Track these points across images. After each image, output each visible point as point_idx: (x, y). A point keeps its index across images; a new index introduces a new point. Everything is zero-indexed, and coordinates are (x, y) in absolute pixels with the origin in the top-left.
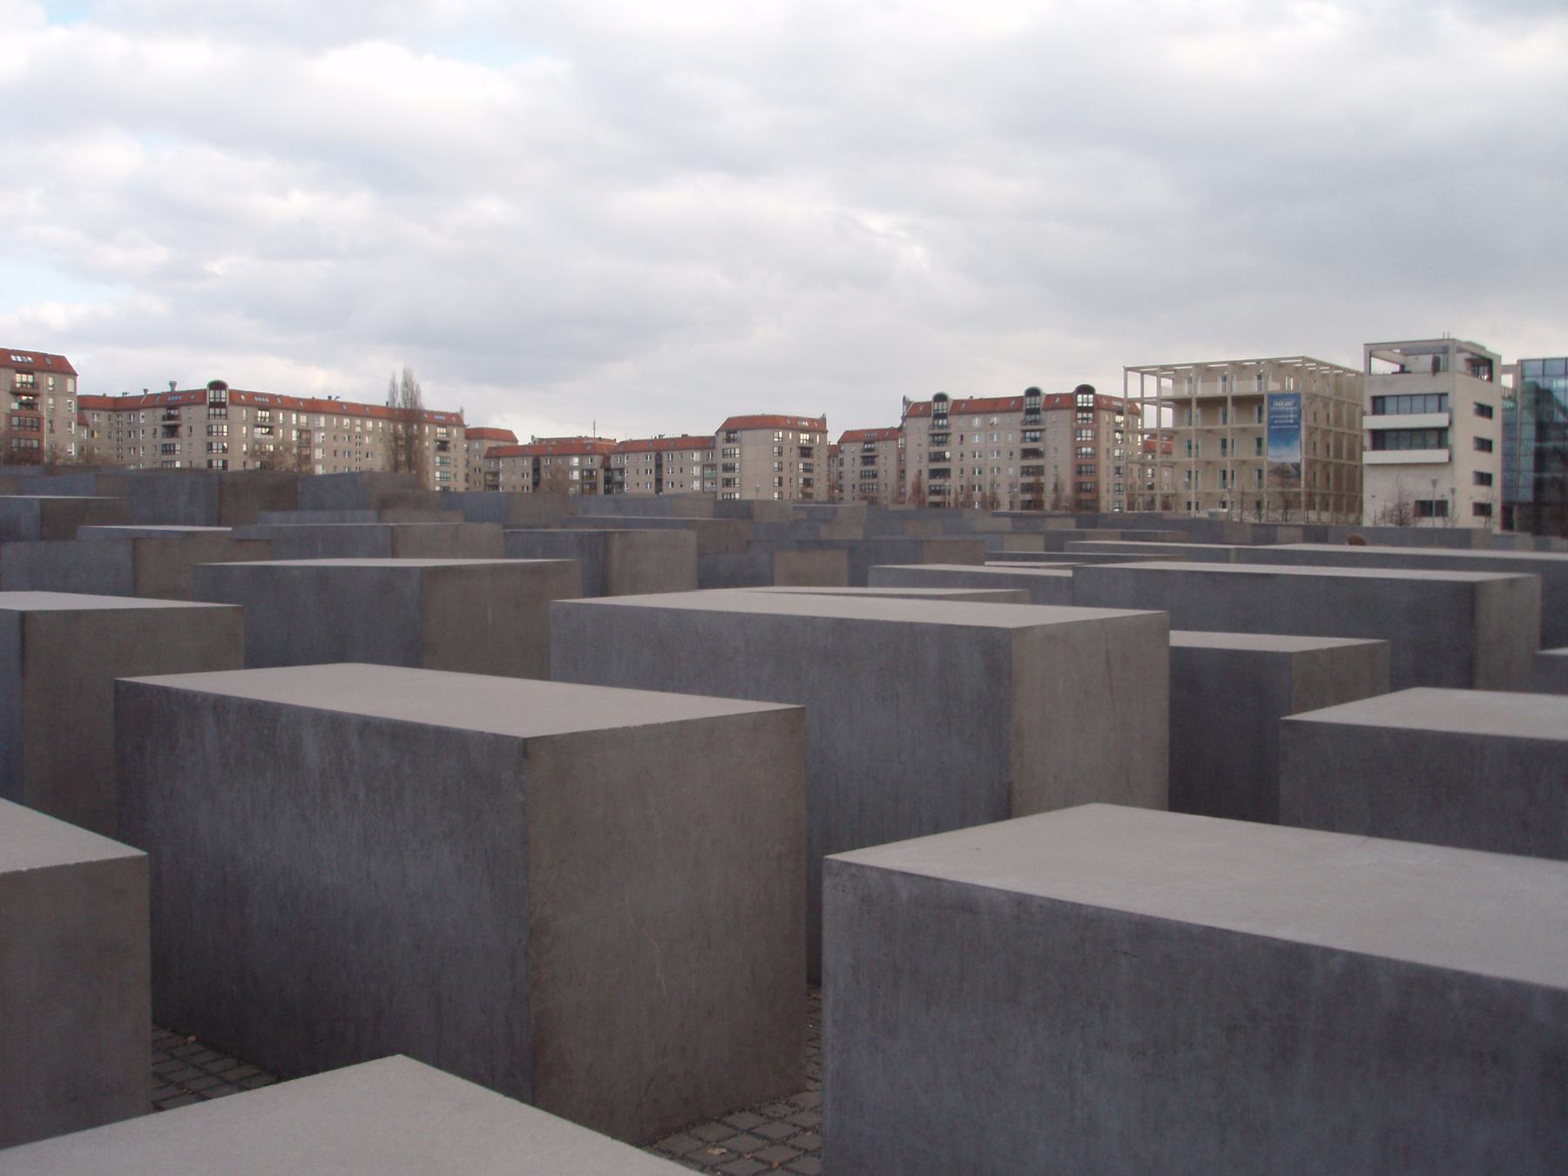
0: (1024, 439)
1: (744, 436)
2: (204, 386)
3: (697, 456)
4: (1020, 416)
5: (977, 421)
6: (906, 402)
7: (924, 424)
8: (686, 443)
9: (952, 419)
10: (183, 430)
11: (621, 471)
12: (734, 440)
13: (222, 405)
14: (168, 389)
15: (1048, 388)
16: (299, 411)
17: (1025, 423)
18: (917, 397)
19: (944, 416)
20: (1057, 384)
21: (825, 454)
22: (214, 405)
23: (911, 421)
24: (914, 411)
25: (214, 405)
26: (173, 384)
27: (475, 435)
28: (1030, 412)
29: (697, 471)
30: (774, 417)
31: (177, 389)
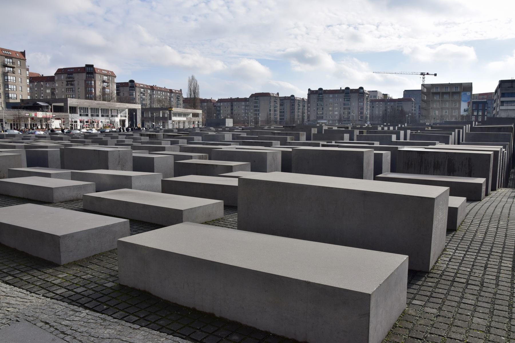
0: (345, 101)
2: (128, 81)
3: (243, 103)
4: (344, 94)
5: (331, 96)
6: (309, 90)
7: (315, 96)
8: (238, 100)
9: (324, 95)
11: (220, 107)
13: (133, 87)
15: (351, 88)
17: (345, 96)
18: (312, 89)
19: (321, 94)
23: (311, 95)
24: (311, 93)
25: (131, 87)
30: (263, 93)
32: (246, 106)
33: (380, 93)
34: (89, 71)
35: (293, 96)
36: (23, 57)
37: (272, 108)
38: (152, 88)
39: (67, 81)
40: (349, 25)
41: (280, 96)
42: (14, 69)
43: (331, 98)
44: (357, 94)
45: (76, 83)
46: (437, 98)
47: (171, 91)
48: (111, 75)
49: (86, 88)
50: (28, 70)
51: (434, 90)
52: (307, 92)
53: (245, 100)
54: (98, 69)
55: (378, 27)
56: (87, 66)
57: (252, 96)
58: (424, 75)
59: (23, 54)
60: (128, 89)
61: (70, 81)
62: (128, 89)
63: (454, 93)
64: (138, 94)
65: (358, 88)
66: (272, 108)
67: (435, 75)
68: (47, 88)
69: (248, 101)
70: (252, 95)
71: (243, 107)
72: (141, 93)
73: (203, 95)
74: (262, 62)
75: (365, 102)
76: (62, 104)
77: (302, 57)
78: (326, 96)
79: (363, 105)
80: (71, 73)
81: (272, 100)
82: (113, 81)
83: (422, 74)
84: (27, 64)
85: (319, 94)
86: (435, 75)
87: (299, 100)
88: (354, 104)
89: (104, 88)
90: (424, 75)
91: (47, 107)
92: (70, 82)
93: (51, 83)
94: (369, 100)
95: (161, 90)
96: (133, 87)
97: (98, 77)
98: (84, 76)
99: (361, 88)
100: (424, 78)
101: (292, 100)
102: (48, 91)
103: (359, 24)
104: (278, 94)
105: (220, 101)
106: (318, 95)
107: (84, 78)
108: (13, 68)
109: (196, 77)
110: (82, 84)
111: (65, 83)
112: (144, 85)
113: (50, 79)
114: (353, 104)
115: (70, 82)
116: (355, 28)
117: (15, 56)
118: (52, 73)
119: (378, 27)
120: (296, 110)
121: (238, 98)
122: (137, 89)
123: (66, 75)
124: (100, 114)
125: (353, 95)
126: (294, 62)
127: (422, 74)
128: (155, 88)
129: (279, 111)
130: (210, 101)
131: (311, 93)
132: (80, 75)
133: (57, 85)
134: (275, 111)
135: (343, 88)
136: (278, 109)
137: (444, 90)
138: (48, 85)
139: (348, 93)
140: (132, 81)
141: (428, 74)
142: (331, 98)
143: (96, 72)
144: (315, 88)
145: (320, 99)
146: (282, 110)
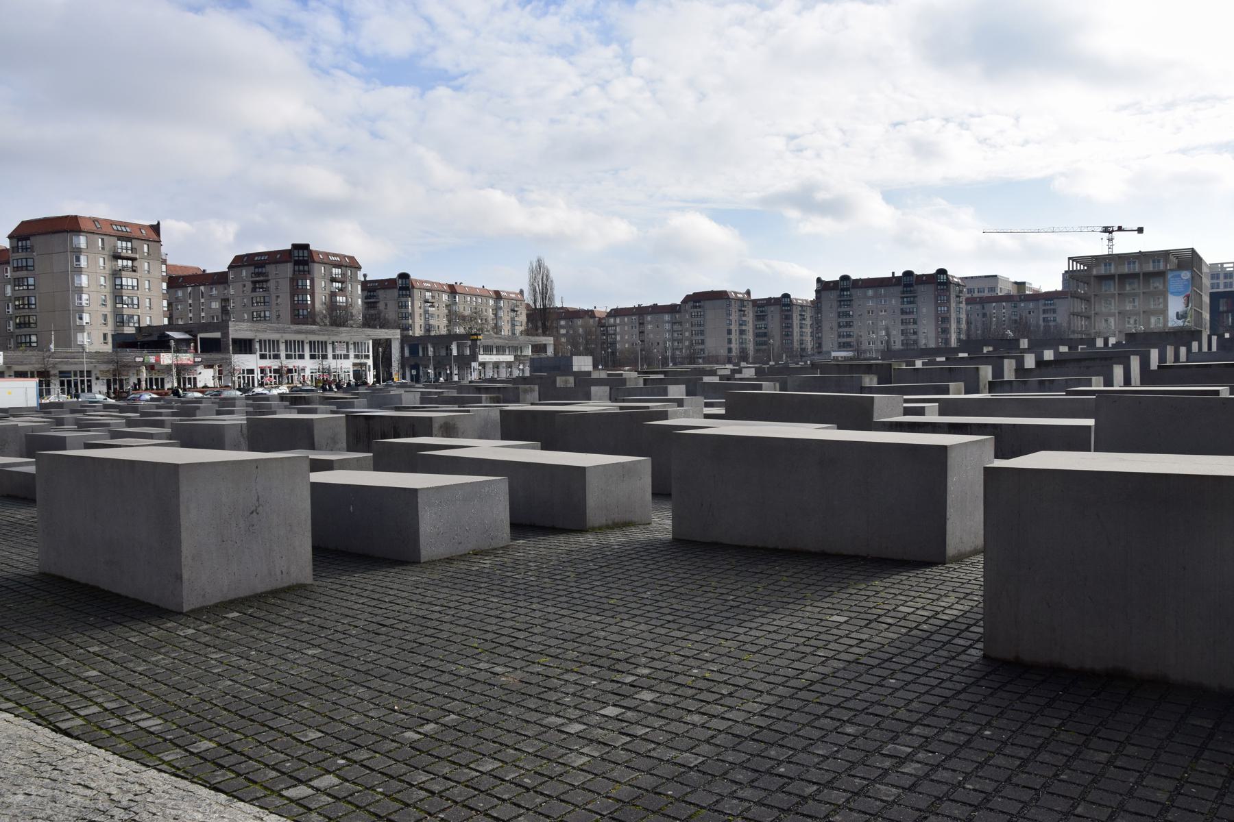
0: (903, 303)
2: (394, 276)
3: (667, 317)
4: (900, 288)
5: (870, 292)
6: (819, 280)
7: (833, 295)
8: (656, 309)
9: (853, 291)
13: (407, 289)
16: (444, 292)
17: (903, 292)
18: (825, 279)
19: (847, 289)
20: (924, 267)
23: (824, 294)
24: (824, 287)
25: (401, 289)
32: (674, 323)
33: (1006, 280)
34: (300, 258)
35: (786, 296)
36: (153, 236)
37: (734, 327)
38: (452, 290)
40: (947, 120)
41: (753, 297)
42: (136, 263)
43: (872, 297)
44: (931, 288)
45: (272, 285)
46: (1112, 289)
47: (498, 295)
48: (351, 264)
49: (292, 296)
50: (164, 262)
51: (1102, 271)
52: (814, 286)
53: (672, 309)
54: (318, 253)
55: (1017, 119)
56: (295, 246)
57: (688, 299)
58: (1111, 232)
59: (156, 228)
60: (395, 292)
61: (259, 282)
62: (395, 292)
63: (1149, 276)
64: (418, 304)
65: (932, 271)
66: (734, 327)
67: (1140, 230)
68: (212, 298)
69: (679, 312)
70: (688, 296)
71: (667, 327)
72: (427, 301)
73: (564, 298)
74: (720, 216)
75: (953, 305)
76: (217, 335)
77: (807, 200)
78: (858, 293)
79: (949, 310)
80: (261, 264)
81: (734, 309)
82: (354, 278)
83: (1107, 230)
84: (163, 250)
85: (843, 290)
86: (1140, 230)
87: (802, 306)
88: (925, 309)
89: (333, 295)
90: (1111, 232)
91: (187, 342)
92: (259, 282)
93: (221, 287)
94: (963, 299)
95: (473, 293)
96: (407, 289)
97: (319, 270)
98: (289, 268)
99: (942, 272)
100: (1110, 240)
101: (785, 305)
102: (215, 305)
103: (972, 116)
104: (748, 293)
105: (616, 313)
106: (838, 292)
107: (290, 275)
108: (133, 259)
109: (549, 263)
110: (286, 286)
111: (249, 286)
112: (432, 283)
113: (219, 279)
114: (924, 310)
115: (259, 282)
116: (961, 125)
117: (137, 234)
118: (219, 263)
119: (1017, 119)
120: (796, 330)
121: (655, 305)
122: (417, 293)
123: (252, 269)
124: (307, 354)
125: (921, 289)
126: (793, 214)
127: (1107, 230)
128: (458, 290)
129: (751, 333)
130: (590, 314)
131: (824, 287)
132: (281, 266)
133: (232, 292)
134: (742, 332)
135: (899, 274)
136: (750, 328)
137: (1125, 269)
138: (214, 292)
139: (911, 285)
140: (404, 276)
141: (1120, 229)
142: (872, 297)
143: (316, 259)
144: (832, 276)
145: (845, 302)
146: (763, 331)
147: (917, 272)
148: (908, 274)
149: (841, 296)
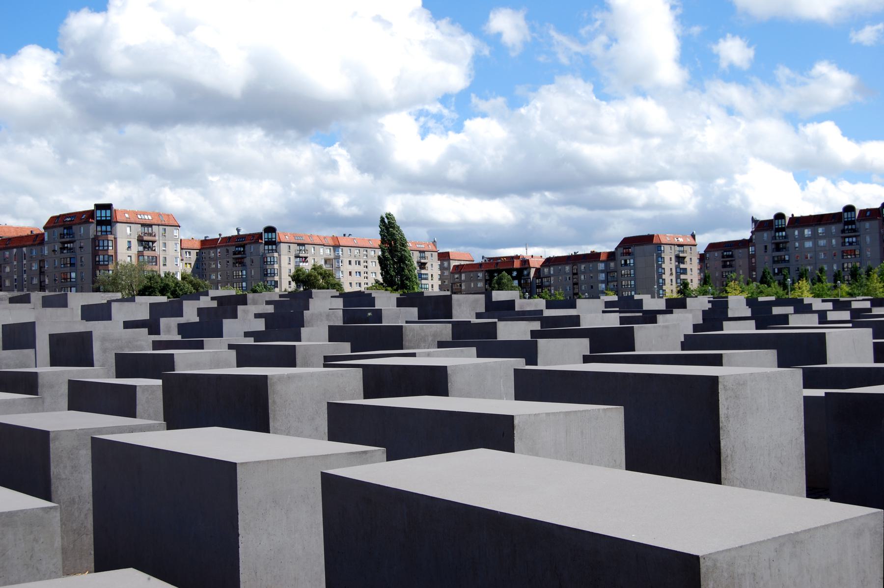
1: (637, 249)
2: (260, 230)
4: (840, 226)
5: (807, 232)
6: (754, 221)
8: (594, 257)
9: (789, 231)
10: (247, 261)
12: (629, 254)
14: (236, 233)
17: (843, 231)
19: (782, 229)
21: (696, 261)
22: (267, 243)
24: (760, 226)
26: (238, 230)
27: (444, 257)
28: (847, 223)
29: (602, 276)
31: (241, 233)
39: (63, 243)
43: (809, 239)
44: (875, 223)
64: (284, 260)
102: (35, 267)
105: (550, 262)
113: (34, 240)
147: (859, 206)
148: (849, 209)
149: (774, 237)
